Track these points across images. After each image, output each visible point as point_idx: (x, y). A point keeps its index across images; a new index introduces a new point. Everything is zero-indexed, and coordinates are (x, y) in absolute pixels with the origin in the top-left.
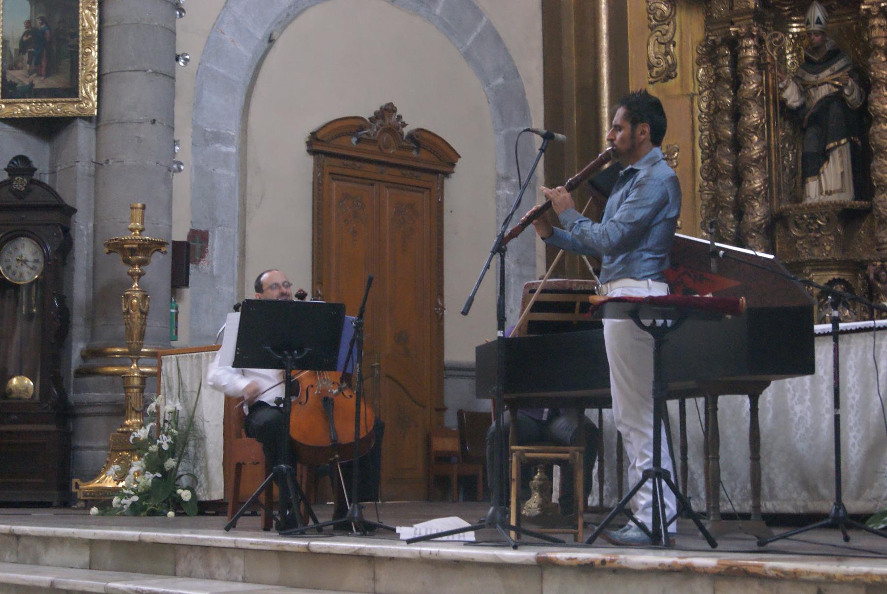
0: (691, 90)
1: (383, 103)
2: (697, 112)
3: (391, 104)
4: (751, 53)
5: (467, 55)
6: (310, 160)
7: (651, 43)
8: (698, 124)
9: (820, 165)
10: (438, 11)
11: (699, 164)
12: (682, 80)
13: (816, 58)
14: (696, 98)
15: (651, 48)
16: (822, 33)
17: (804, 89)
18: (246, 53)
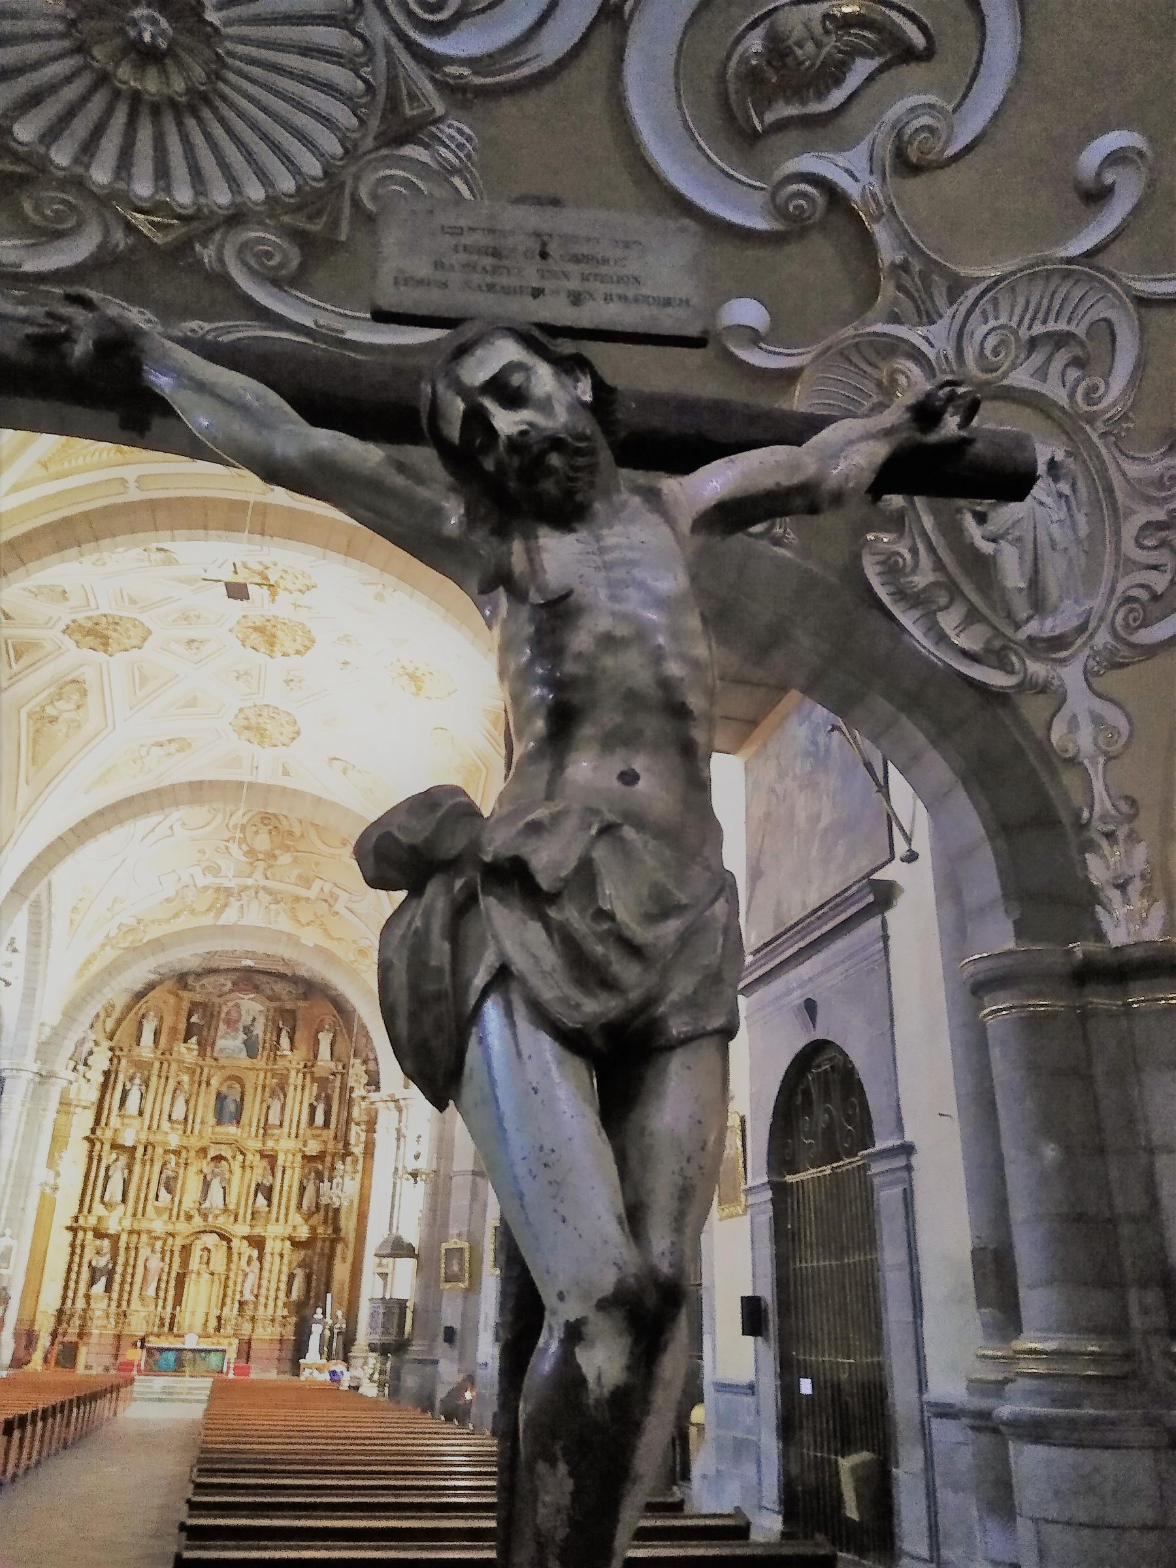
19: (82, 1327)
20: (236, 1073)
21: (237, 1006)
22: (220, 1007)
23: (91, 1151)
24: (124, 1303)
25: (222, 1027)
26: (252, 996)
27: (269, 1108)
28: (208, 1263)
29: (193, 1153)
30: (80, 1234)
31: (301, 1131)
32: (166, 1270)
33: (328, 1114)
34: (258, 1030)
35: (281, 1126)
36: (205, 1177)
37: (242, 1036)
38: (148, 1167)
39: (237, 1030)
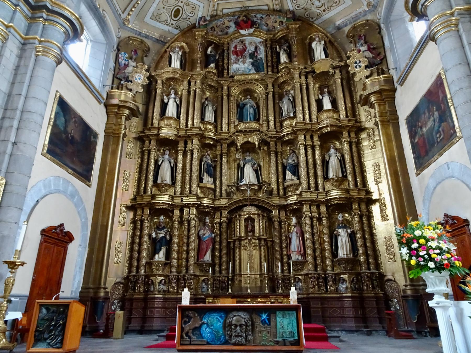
0: (128, 229)
1: (61, 223)
2: (129, 235)
3: (63, 224)
4: (146, 224)
5: (78, 212)
6: (40, 236)
7: (121, 217)
8: (129, 238)
9: (159, 252)
10: (75, 200)
11: (127, 247)
12: (126, 227)
13: (160, 227)
14: (129, 232)
15: (121, 218)
16: (162, 222)
17: (157, 234)
18: (32, 205)
19: (147, 292)
20: (249, 86)
21: (242, 42)
22: (228, 44)
23: (142, 148)
24: (184, 269)
25: (233, 57)
26: (252, 30)
27: (281, 109)
28: (253, 231)
29: (225, 146)
30: (139, 212)
31: (314, 116)
32: (218, 240)
33: (334, 102)
34: (262, 55)
35: (295, 117)
36: (239, 165)
37: (249, 61)
38: (189, 157)
39: (245, 57)
